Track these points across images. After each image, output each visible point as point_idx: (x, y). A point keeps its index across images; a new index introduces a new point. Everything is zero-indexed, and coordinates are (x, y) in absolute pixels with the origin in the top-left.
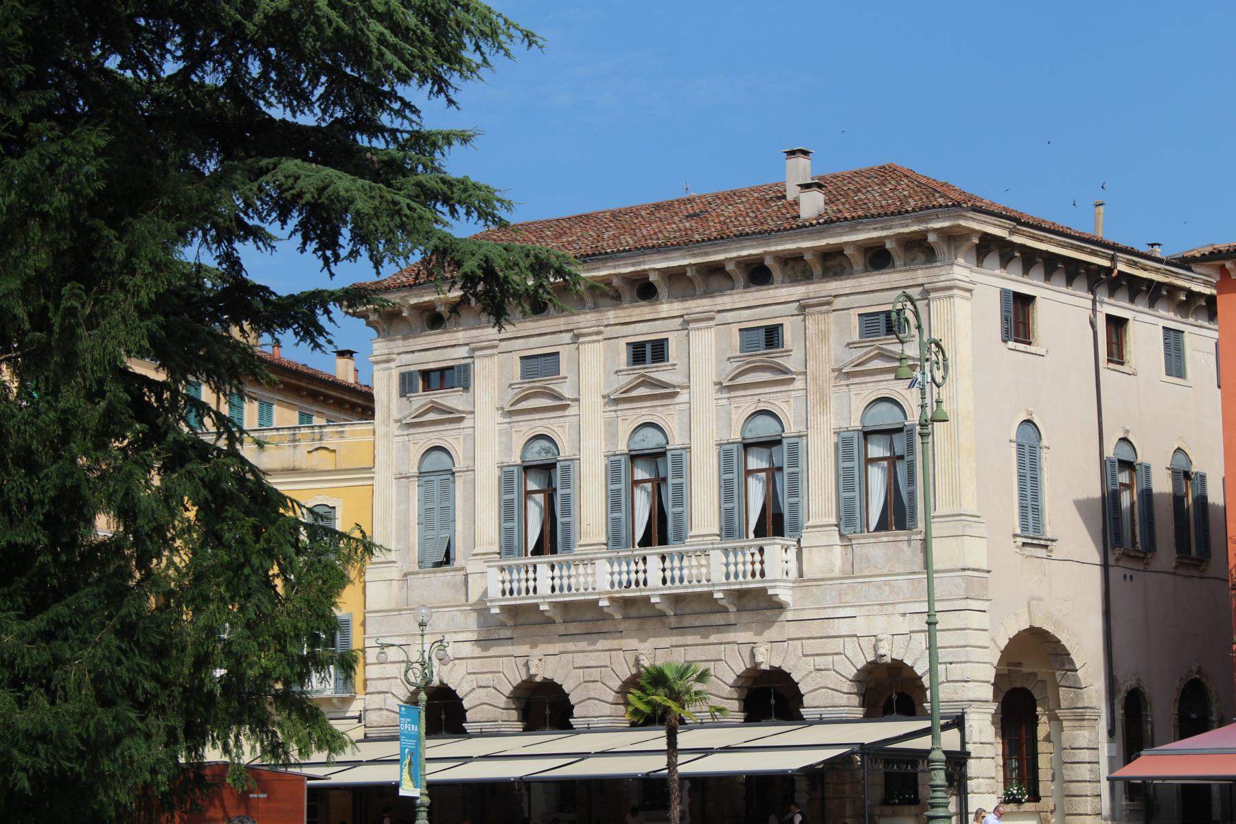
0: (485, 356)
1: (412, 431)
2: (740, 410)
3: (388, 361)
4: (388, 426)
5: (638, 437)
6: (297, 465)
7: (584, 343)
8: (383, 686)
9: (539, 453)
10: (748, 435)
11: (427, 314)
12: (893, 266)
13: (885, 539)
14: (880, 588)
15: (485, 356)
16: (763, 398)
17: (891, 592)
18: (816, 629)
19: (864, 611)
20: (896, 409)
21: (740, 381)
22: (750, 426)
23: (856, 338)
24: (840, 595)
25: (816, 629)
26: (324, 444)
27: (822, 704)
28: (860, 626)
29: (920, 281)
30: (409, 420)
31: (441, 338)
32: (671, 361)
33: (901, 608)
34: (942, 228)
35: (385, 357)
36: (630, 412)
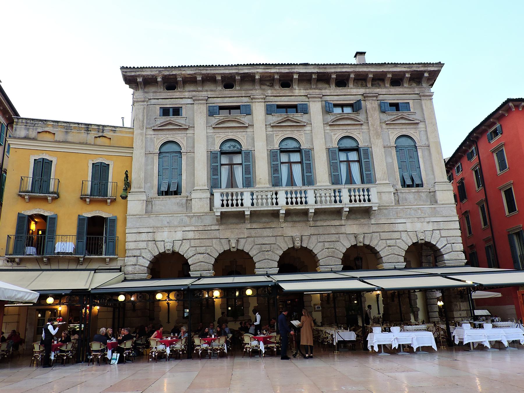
0: (200, 104)
1: (156, 133)
3: (144, 101)
4: (143, 129)
5: (284, 143)
6: (89, 142)
7: (255, 102)
8: (137, 253)
9: (229, 147)
10: (340, 146)
11: (166, 84)
12: (403, 86)
13: (413, 191)
14: (416, 210)
15: (200, 104)
16: (349, 131)
18: (386, 228)
19: (410, 220)
20: (410, 140)
21: (338, 123)
22: (341, 142)
24: (397, 213)
26: (104, 134)
27: (392, 261)
28: (409, 227)
29: (417, 92)
31: (176, 94)
33: (427, 220)
35: (143, 99)
36: (280, 132)
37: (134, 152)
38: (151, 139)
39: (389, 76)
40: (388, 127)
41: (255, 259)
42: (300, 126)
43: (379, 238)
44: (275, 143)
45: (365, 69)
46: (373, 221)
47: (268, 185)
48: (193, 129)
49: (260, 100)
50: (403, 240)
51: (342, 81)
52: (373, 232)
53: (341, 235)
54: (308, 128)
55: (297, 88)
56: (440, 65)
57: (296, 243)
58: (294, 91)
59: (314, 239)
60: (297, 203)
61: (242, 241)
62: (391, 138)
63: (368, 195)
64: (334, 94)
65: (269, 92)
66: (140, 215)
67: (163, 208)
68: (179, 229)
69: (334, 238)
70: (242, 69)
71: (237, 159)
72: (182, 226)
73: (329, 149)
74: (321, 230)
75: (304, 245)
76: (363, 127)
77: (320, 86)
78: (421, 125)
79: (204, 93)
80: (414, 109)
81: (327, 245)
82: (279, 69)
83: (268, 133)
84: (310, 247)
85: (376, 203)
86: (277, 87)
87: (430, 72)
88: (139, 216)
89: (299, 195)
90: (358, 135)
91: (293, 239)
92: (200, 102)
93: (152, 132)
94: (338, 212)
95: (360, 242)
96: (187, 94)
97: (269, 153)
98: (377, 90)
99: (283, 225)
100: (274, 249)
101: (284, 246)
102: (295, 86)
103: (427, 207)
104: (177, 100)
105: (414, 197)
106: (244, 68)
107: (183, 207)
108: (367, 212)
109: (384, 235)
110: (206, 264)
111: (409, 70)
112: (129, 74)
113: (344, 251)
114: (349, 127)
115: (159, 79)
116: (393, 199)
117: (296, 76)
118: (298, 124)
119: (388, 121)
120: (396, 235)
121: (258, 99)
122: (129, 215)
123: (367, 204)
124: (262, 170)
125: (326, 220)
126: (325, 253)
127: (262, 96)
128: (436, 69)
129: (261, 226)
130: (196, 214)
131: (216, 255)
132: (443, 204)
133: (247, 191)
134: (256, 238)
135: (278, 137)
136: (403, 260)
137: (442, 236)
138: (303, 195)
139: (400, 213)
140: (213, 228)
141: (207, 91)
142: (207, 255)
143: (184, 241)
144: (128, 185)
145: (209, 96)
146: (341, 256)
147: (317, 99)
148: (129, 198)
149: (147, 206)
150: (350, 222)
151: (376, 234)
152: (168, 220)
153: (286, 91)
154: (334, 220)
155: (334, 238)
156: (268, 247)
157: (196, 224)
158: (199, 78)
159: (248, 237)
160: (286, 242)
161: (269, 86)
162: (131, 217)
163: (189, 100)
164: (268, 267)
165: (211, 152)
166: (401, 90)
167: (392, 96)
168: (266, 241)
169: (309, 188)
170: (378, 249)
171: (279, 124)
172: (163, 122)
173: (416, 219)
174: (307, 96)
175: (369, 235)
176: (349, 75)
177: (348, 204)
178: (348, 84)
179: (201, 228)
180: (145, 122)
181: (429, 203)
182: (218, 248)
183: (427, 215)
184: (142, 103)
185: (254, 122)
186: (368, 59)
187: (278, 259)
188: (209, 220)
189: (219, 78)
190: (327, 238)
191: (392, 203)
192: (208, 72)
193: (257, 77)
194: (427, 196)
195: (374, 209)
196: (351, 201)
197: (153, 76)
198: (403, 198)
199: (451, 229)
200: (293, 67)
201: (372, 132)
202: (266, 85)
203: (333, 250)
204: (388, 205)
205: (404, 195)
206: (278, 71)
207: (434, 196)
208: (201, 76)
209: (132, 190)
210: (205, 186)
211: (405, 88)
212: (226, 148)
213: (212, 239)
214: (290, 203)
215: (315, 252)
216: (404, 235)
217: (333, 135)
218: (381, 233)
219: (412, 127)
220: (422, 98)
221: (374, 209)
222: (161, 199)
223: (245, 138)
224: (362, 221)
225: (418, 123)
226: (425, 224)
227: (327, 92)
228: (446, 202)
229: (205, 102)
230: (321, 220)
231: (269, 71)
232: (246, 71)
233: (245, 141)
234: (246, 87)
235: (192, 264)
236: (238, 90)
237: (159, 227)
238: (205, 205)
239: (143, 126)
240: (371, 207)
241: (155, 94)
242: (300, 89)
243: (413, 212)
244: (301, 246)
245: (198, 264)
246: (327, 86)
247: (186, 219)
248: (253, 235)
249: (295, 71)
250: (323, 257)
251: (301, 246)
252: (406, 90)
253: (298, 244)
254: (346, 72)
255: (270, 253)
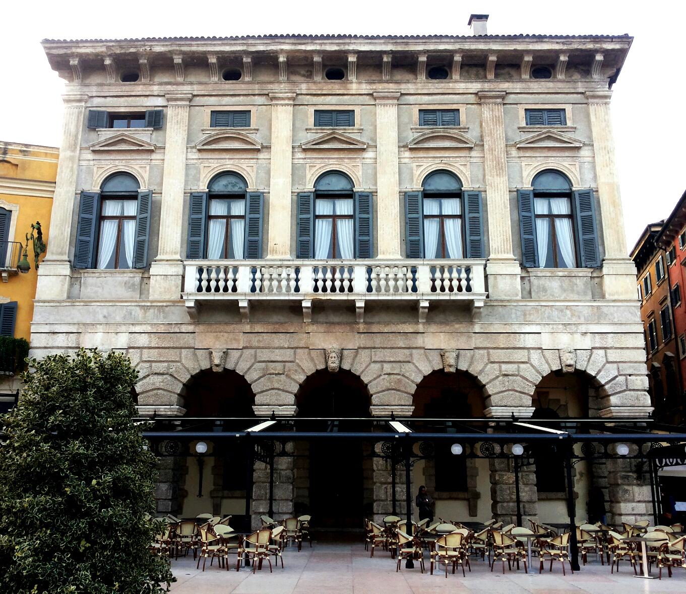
0: (178, 106)
1: (97, 157)
2: (422, 168)
4: (74, 151)
7: (277, 105)
9: (226, 186)
10: (427, 188)
12: (555, 77)
13: (561, 274)
14: (562, 311)
15: (178, 106)
17: (573, 315)
18: (502, 341)
19: (548, 329)
20: (561, 180)
21: (426, 145)
22: (429, 181)
23: (523, 124)
24: (525, 315)
25: (502, 341)
27: (509, 404)
28: (546, 341)
29: (581, 90)
30: (97, 148)
32: (357, 126)
33: (583, 329)
34: (613, 50)
35: (78, 97)
37: (57, 190)
38: (88, 167)
39: (528, 58)
40: (521, 154)
41: (255, 388)
42: (355, 149)
43: (486, 360)
44: (307, 180)
45: (482, 46)
46: (477, 328)
47: (288, 257)
48: (162, 151)
49: (287, 102)
50: (532, 365)
51: (439, 67)
52: (476, 348)
53: (414, 351)
54: (369, 154)
55: (354, 80)
56: (626, 39)
57: (330, 362)
58: (349, 86)
59: (364, 354)
60: (333, 289)
61: (234, 355)
62: (525, 174)
63: (468, 280)
64: (424, 91)
65: (304, 88)
66: (58, 302)
67: (100, 290)
68: (123, 328)
69: (401, 355)
70: (254, 45)
71: (239, 208)
72: (129, 324)
73: (405, 193)
74: (378, 341)
75: (346, 366)
76: (473, 154)
77: (398, 76)
78: (585, 152)
79: (187, 88)
80: (574, 122)
81: (387, 368)
82: (321, 44)
83: (296, 161)
84: (357, 370)
85: (481, 295)
86: (318, 78)
87: (606, 53)
88: (55, 303)
89: (338, 276)
90: (462, 168)
91: (325, 354)
92: (179, 103)
93: (91, 156)
94: (410, 309)
95: (450, 366)
96: (156, 89)
97: (295, 198)
98: (505, 86)
99: (310, 328)
100: (289, 370)
101: (309, 366)
102: (352, 77)
103: (585, 306)
104: (138, 99)
105: (561, 287)
106: (258, 42)
107: (134, 290)
108: (465, 310)
109: (497, 355)
110: (165, 393)
111: (565, 47)
112: (55, 52)
113: (419, 379)
114: (447, 154)
115: (108, 62)
116: (519, 287)
117: (352, 59)
118: (352, 147)
119: (520, 142)
120: (520, 355)
121: (283, 99)
122: (39, 301)
123: (464, 296)
124: (280, 229)
125: (387, 324)
126: (384, 382)
127: (290, 95)
128: (617, 46)
129: (270, 328)
130: (154, 304)
131: (185, 378)
132: (614, 301)
133: (245, 265)
134: (258, 351)
135: (314, 169)
136: (530, 402)
137: (610, 359)
138: (346, 275)
139: (530, 314)
140: (184, 328)
141: (191, 84)
142: (169, 378)
143: (130, 351)
144: (41, 246)
145: (195, 93)
146: (413, 389)
147: (390, 101)
148: (41, 271)
149: (71, 285)
150: (433, 328)
151: (481, 352)
152: (105, 311)
153: (335, 86)
154: (404, 323)
155: (401, 355)
156: (279, 367)
157: (155, 322)
158: (178, 60)
159: (244, 348)
160: (312, 360)
161: (304, 76)
162: (41, 304)
163: (160, 99)
164: (276, 402)
165: (191, 194)
166: (551, 85)
167: (533, 96)
168: (277, 355)
169: (357, 263)
170: (483, 379)
171: (317, 147)
172: (111, 138)
173: (560, 326)
174: (371, 95)
175: (469, 353)
176: (452, 57)
177: (428, 295)
178: (451, 74)
179: (162, 329)
180: (80, 137)
181: (589, 297)
182: (190, 365)
183: (582, 320)
184: (78, 104)
185: (273, 141)
186: (492, 28)
187: (295, 388)
188: (177, 316)
189: (213, 60)
190: (388, 355)
191: (517, 295)
192: (194, 49)
193: (282, 59)
194: (586, 284)
195: (477, 304)
196: (434, 289)
197: (97, 55)
198: (538, 287)
199: (628, 348)
200: (347, 41)
201: (488, 163)
202: (299, 74)
203: (399, 377)
204: (508, 298)
205: (542, 282)
206: (318, 48)
207: (601, 285)
208: (181, 57)
209: (49, 256)
210: (176, 253)
211: (560, 81)
212: (219, 187)
213: (181, 348)
214: (320, 289)
215: (365, 379)
216: (535, 357)
217: (415, 168)
218: (491, 351)
219: (567, 154)
220: (590, 100)
221: (477, 304)
222: (97, 275)
223: (255, 170)
224: (457, 326)
225: (579, 148)
226: (578, 337)
227: (410, 88)
228: (622, 297)
229: (188, 103)
230: (379, 323)
231: (303, 47)
232: (261, 48)
233: (253, 175)
234: (264, 77)
235: (142, 393)
236: (248, 83)
237: (88, 324)
238: (174, 288)
239: (75, 144)
240: (472, 301)
241: (100, 89)
242: (360, 83)
243: (555, 313)
244: (340, 367)
245: (151, 393)
246: (410, 77)
247: (138, 313)
248: (255, 344)
249: (351, 47)
250: (379, 389)
251: (340, 367)
252: (560, 85)
253: (333, 364)
254: (446, 51)
255: (283, 377)
